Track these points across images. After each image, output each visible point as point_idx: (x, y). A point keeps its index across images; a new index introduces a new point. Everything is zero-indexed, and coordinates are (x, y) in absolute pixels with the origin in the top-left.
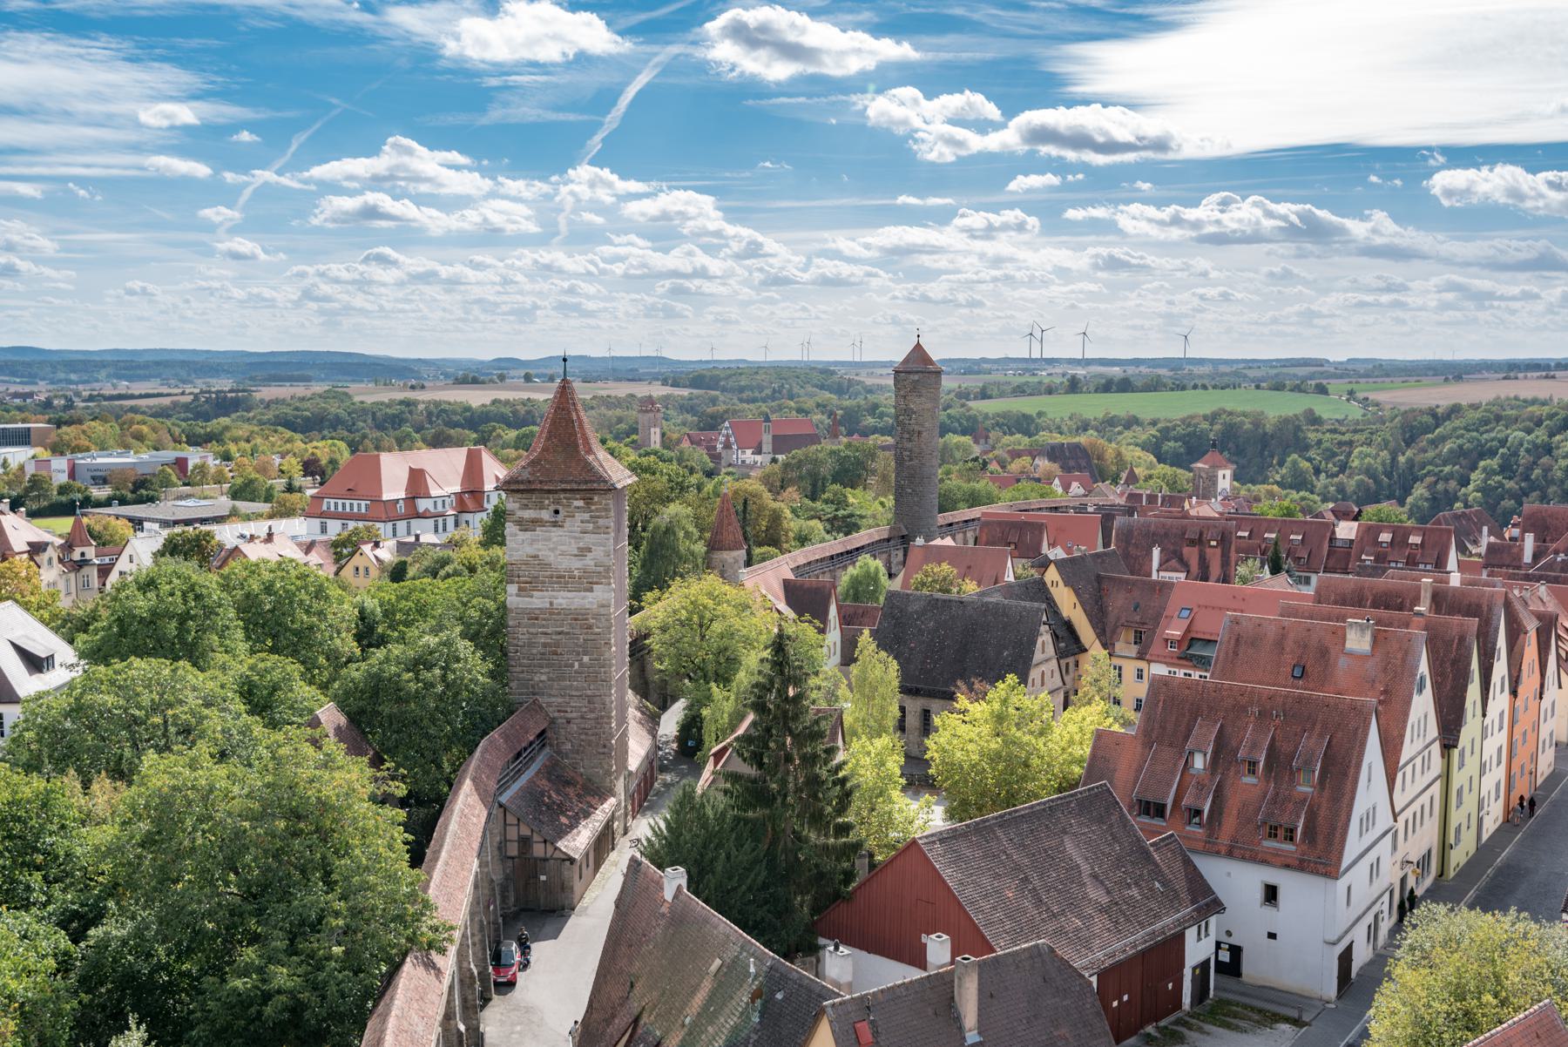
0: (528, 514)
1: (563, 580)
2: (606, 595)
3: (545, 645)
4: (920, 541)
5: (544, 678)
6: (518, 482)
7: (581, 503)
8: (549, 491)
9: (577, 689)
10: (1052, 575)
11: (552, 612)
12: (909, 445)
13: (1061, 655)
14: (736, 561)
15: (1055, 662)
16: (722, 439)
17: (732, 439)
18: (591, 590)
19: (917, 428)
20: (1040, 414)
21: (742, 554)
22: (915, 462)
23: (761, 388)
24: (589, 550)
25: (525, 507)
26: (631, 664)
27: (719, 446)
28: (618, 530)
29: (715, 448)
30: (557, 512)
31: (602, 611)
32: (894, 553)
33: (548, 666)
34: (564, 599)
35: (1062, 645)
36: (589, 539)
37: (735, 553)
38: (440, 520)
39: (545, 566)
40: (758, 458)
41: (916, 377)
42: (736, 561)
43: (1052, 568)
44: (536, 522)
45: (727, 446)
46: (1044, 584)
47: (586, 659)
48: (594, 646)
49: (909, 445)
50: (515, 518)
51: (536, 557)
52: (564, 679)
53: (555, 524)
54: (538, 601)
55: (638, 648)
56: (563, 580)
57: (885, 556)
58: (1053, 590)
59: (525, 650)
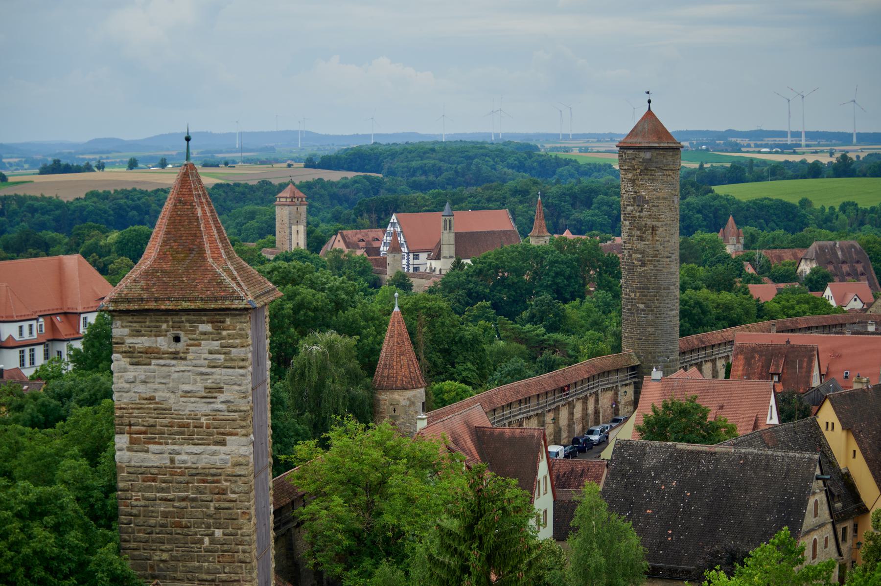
0: (143, 342)
1: (188, 430)
2: (243, 450)
3: (165, 515)
4: (657, 374)
5: (165, 556)
6: (128, 301)
7: (208, 327)
8: (167, 312)
9: (208, 572)
10: (827, 415)
11: (172, 469)
12: (640, 245)
13: (837, 518)
14: (412, 403)
15: (829, 527)
16: (387, 238)
17: (401, 239)
18: (223, 443)
19: (649, 222)
20: (805, 203)
21: (419, 394)
22: (649, 267)
23: (439, 171)
24: (220, 390)
25: (137, 333)
26: (276, 540)
27: (384, 249)
28: (258, 362)
29: (377, 251)
30: (177, 339)
31: (238, 471)
32: (621, 390)
33: (170, 542)
34: (189, 455)
35: (839, 505)
36: (220, 375)
37: (410, 394)
38: (27, 350)
39: (163, 411)
40: (436, 264)
41: (648, 155)
42: (412, 403)
43: (827, 405)
44: (151, 354)
45: (395, 248)
46: (818, 427)
47: (218, 533)
48: (226, 517)
49: (640, 245)
50: (124, 348)
51: (151, 399)
52: (192, 559)
53: (175, 356)
54: (154, 457)
55: (286, 520)
56: (188, 430)
57: (610, 394)
58: (828, 435)
59: (140, 520)
